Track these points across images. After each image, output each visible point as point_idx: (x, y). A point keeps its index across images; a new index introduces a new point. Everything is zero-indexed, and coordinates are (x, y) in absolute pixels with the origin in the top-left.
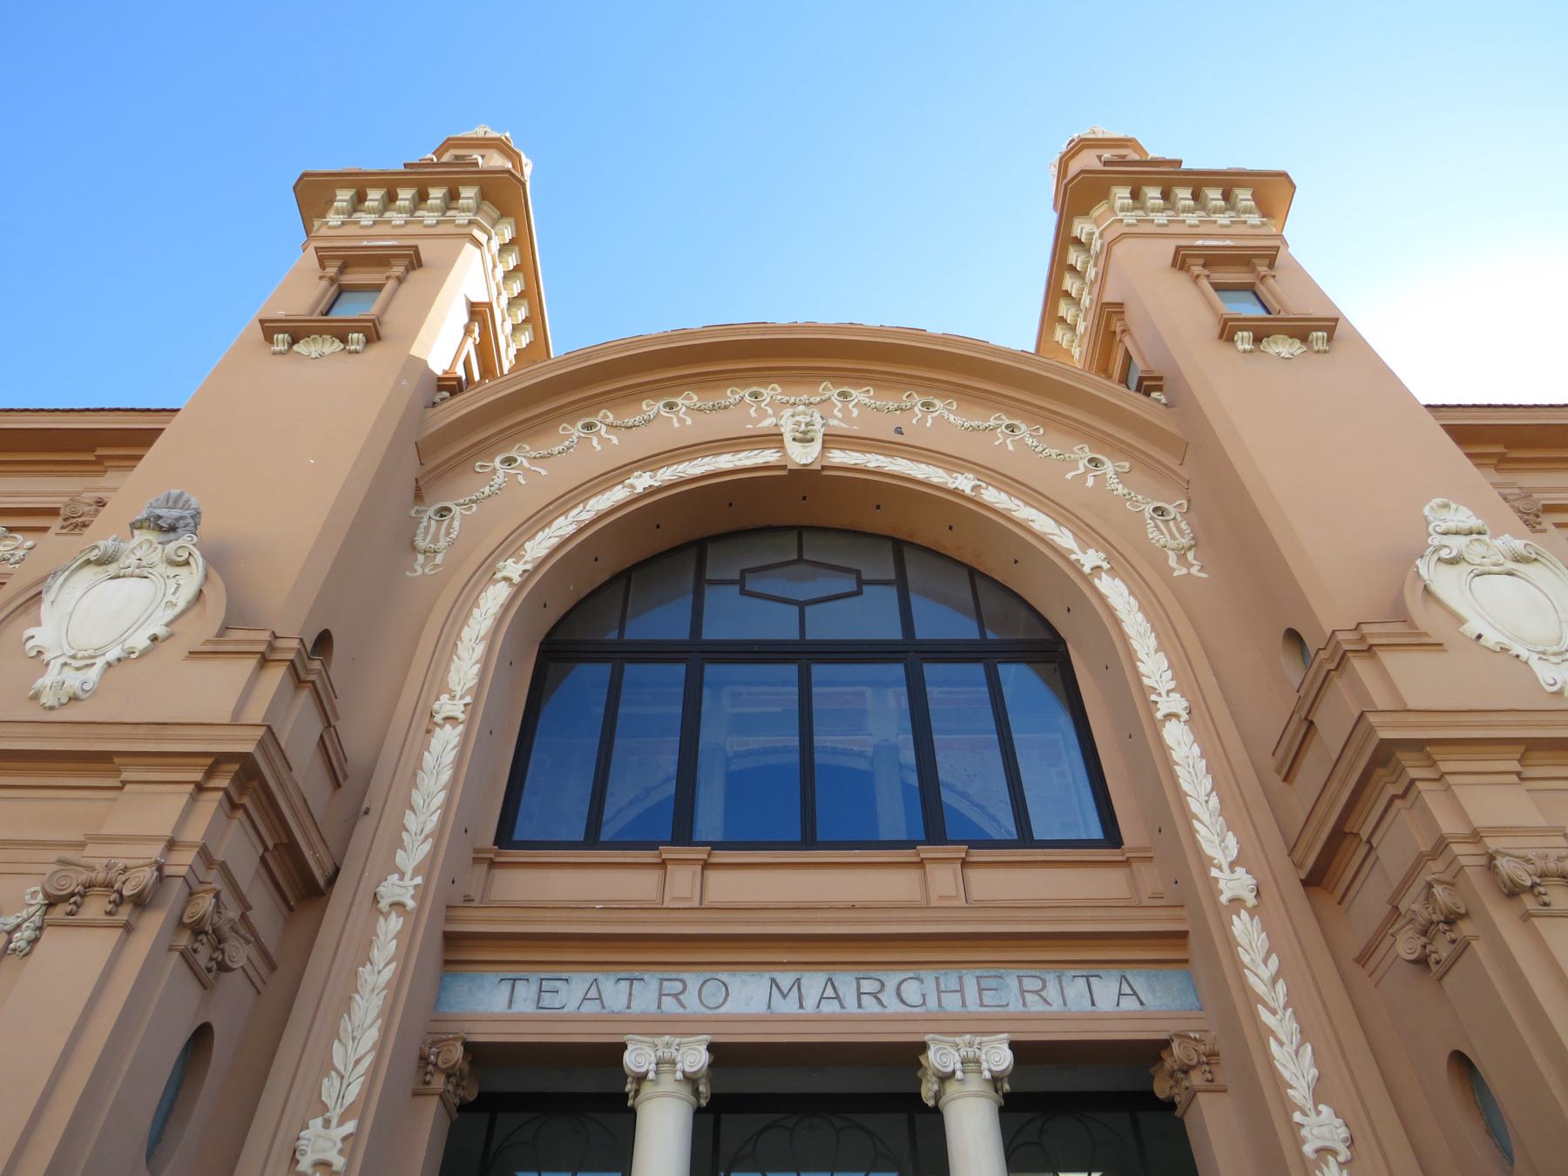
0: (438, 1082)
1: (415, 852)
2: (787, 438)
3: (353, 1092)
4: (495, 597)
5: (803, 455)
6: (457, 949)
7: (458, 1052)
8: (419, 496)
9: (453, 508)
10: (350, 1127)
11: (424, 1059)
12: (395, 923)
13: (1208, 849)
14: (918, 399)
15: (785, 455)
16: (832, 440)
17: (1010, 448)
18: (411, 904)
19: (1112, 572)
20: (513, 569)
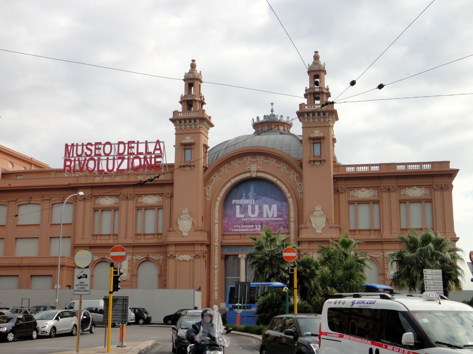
0: (223, 259)
1: (217, 240)
2: (251, 171)
3: (217, 263)
4: (218, 204)
5: (254, 175)
6: (223, 246)
7: (224, 256)
8: (205, 186)
9: (210, 187)
10: (218, 265)
11: (221, 257)
12: (217, 247)
13: (291, 238)
14: (271, 159)
15: (251, 175)
16: (257, 171)
17: (283, 171)
18: (218, 245)
19: (291, 197)
20: (219, 199)
